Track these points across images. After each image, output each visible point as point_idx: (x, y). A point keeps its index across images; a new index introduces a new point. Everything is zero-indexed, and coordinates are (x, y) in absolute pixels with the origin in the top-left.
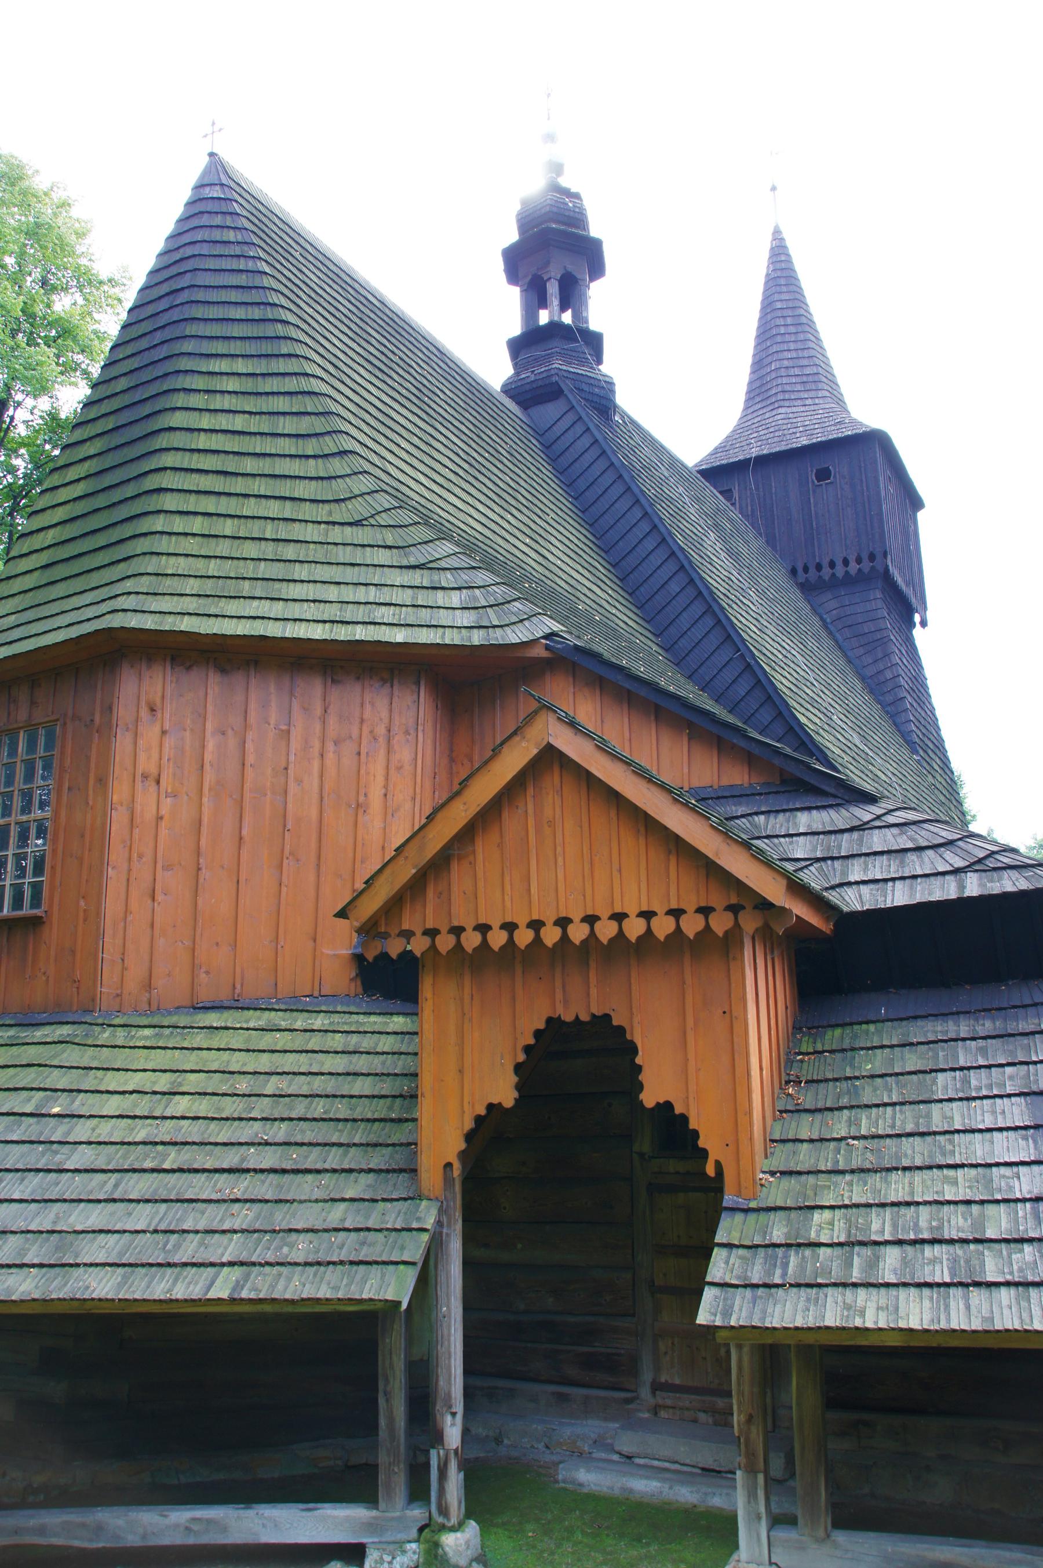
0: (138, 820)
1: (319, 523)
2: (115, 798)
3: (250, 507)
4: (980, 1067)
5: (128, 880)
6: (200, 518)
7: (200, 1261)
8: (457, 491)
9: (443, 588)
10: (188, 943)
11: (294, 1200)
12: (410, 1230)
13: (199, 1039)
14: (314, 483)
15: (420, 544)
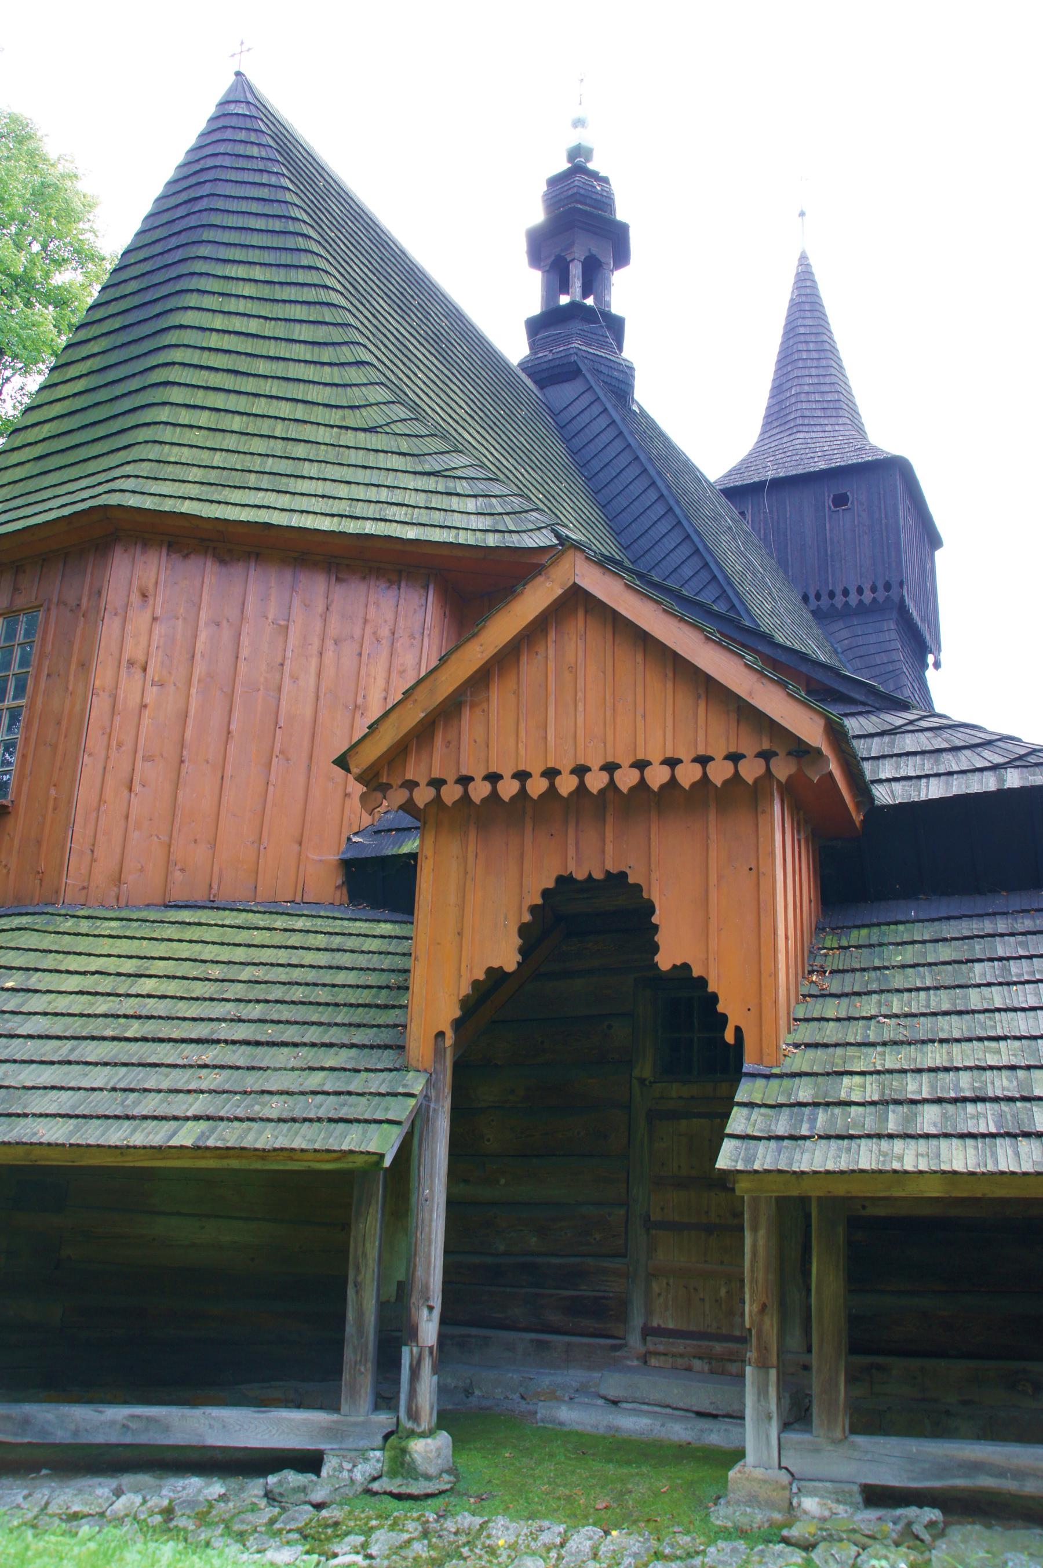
0: (120, 706)
1: (332, 426)
2: (98, 683)
3: (260, 406)
4: (1020, 957)
5: (105, 768)
6: (207, 413)
7: (162, 1114)
8: (471, 431)
9: (458, 495)
10: (164, 838)
11: (268, 1068)
12: (395, 1095)
14: (328, 389)
15: (436, 453)
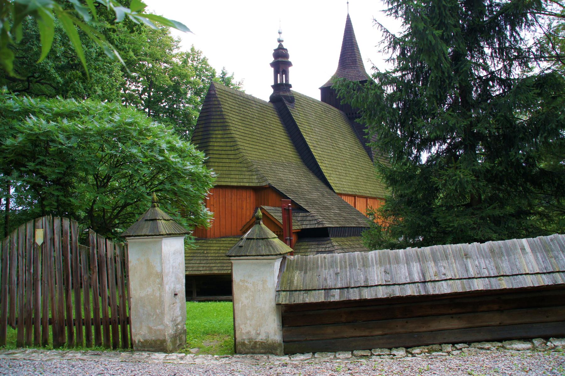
3: (224, 161)
13: (222, 242)
